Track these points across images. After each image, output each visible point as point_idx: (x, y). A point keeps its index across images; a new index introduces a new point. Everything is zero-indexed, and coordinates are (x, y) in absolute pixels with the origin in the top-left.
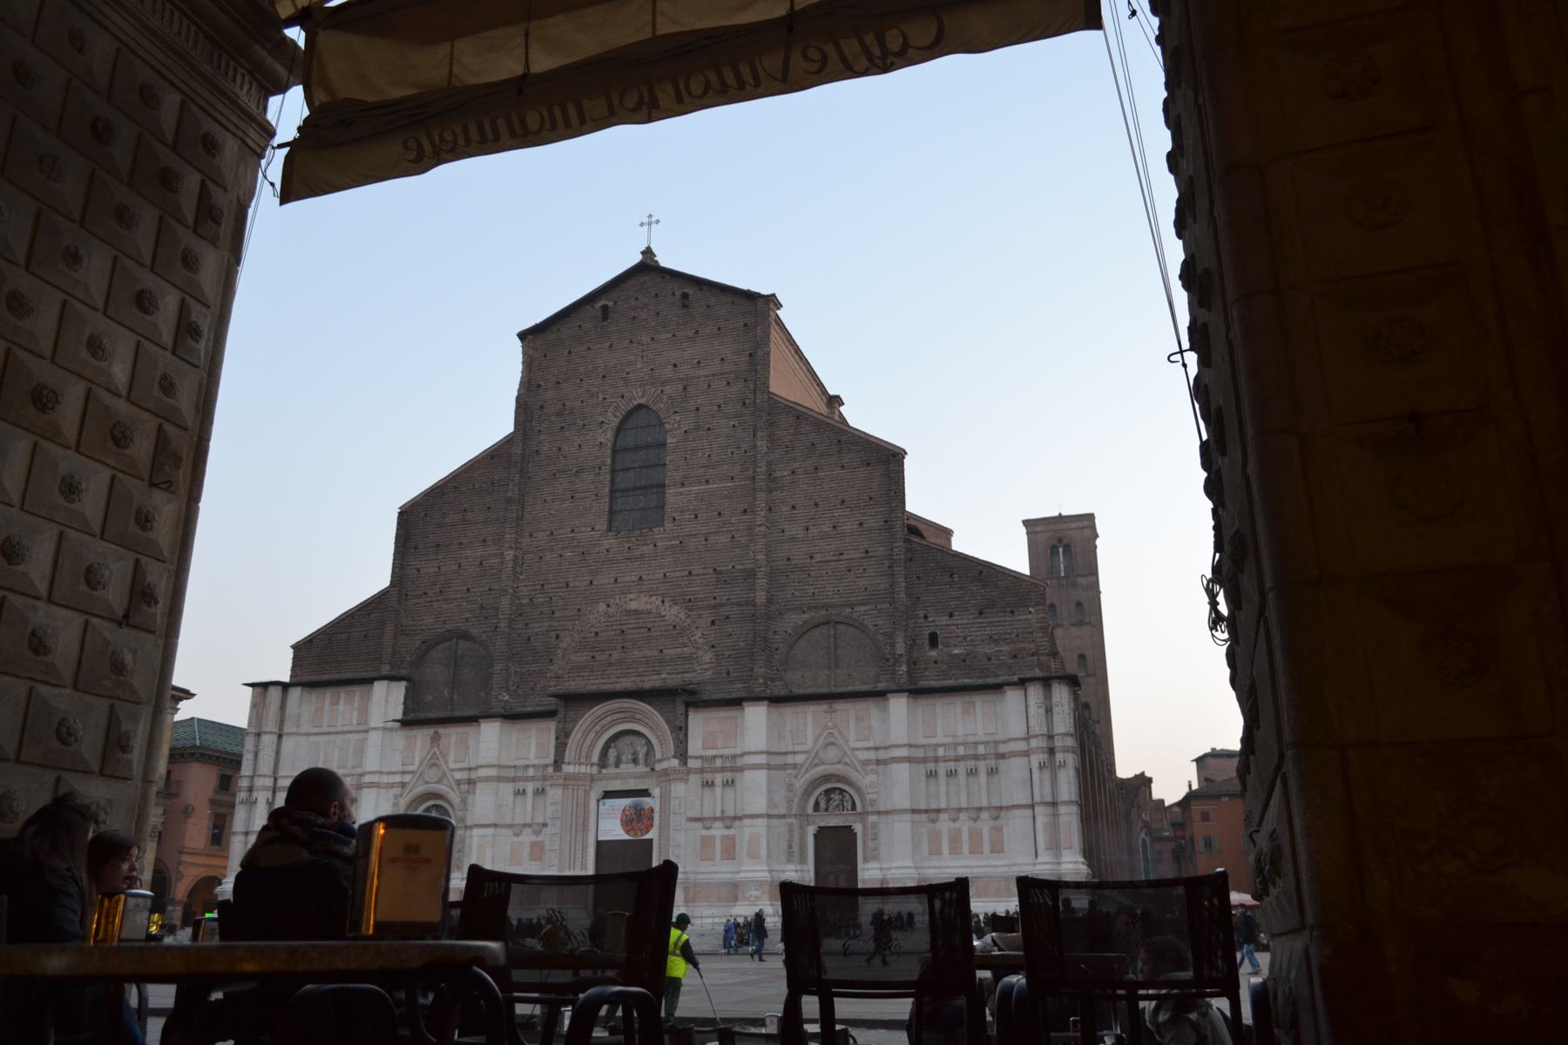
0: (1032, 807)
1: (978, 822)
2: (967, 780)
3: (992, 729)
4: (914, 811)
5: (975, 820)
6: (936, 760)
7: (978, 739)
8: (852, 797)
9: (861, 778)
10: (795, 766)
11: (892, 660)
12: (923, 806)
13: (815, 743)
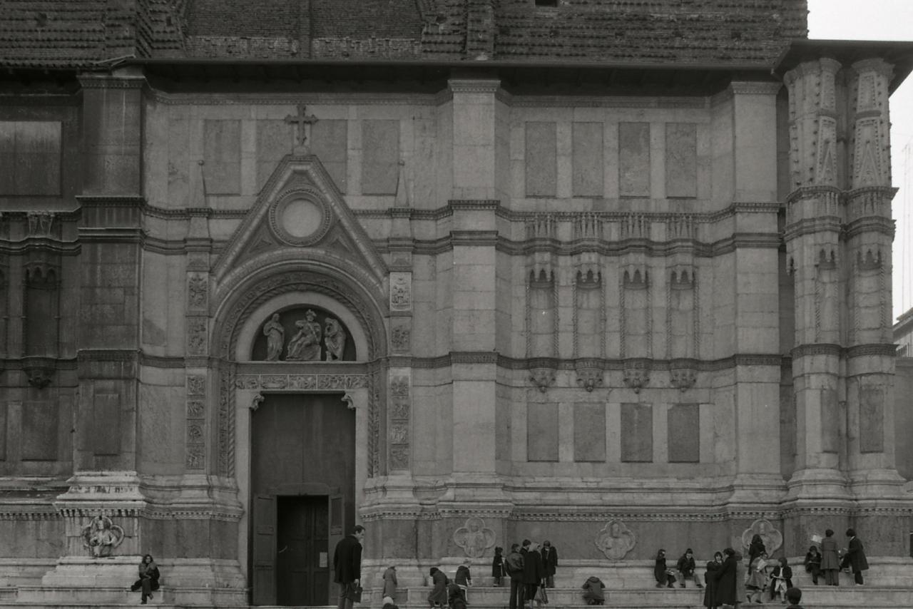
0: (784, 362)
1: (644, 393)
2: (622, 296)
3: (683, 189)
4: (504, 361)
5: (638, 388)
6: (555, 248)
7: (653, 209)
8: (341, 323)
9: (373, 281)
10: (210, 245)
11: (450, 20)
12: (518, 351)
13: (262, 195)
